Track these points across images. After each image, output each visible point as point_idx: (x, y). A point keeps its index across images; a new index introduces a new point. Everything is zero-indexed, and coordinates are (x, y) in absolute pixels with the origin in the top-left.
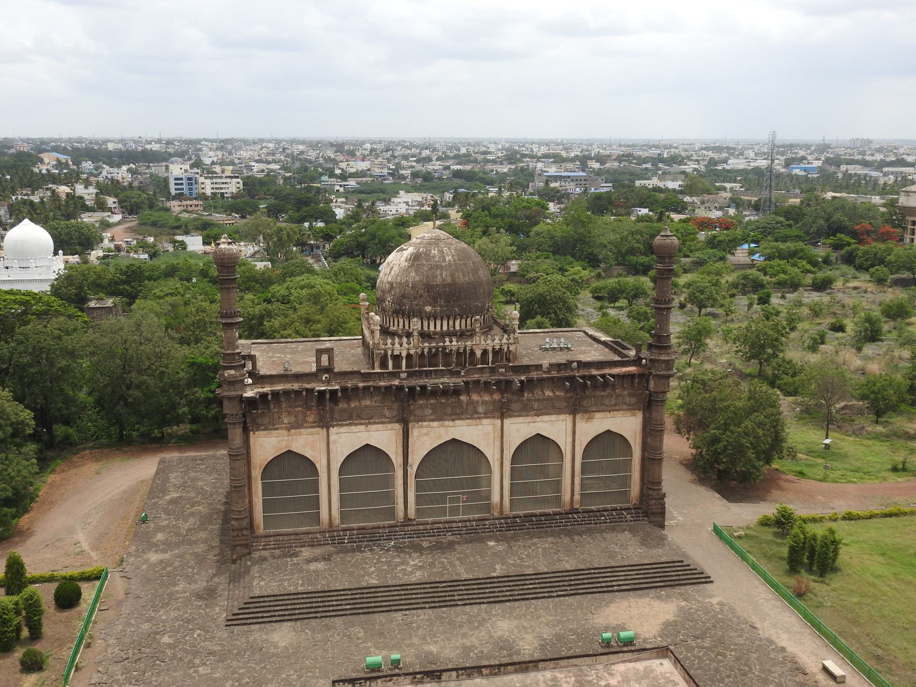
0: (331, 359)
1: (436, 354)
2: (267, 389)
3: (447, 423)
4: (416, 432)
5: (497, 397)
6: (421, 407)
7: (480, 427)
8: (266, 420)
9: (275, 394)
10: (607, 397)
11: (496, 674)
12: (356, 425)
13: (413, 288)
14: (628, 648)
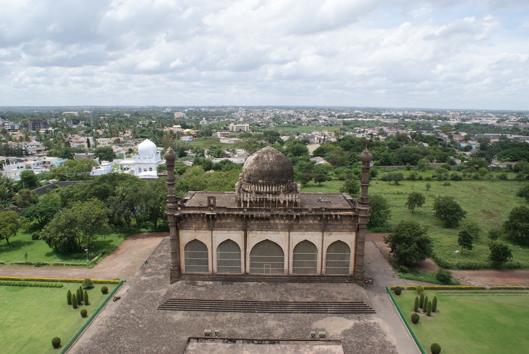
0: (215, 202)
1: (263, 202)
2: (187, 212)
3: (264, 232)
4: (250, 235)
5: (287, 222)
6: (252, 224)
7: (279, 235)
8: (186, 225)
9: (189, 215)
10: (339, 225)
11: (260, 344)
13: (254, 172)
14: (324, 339)
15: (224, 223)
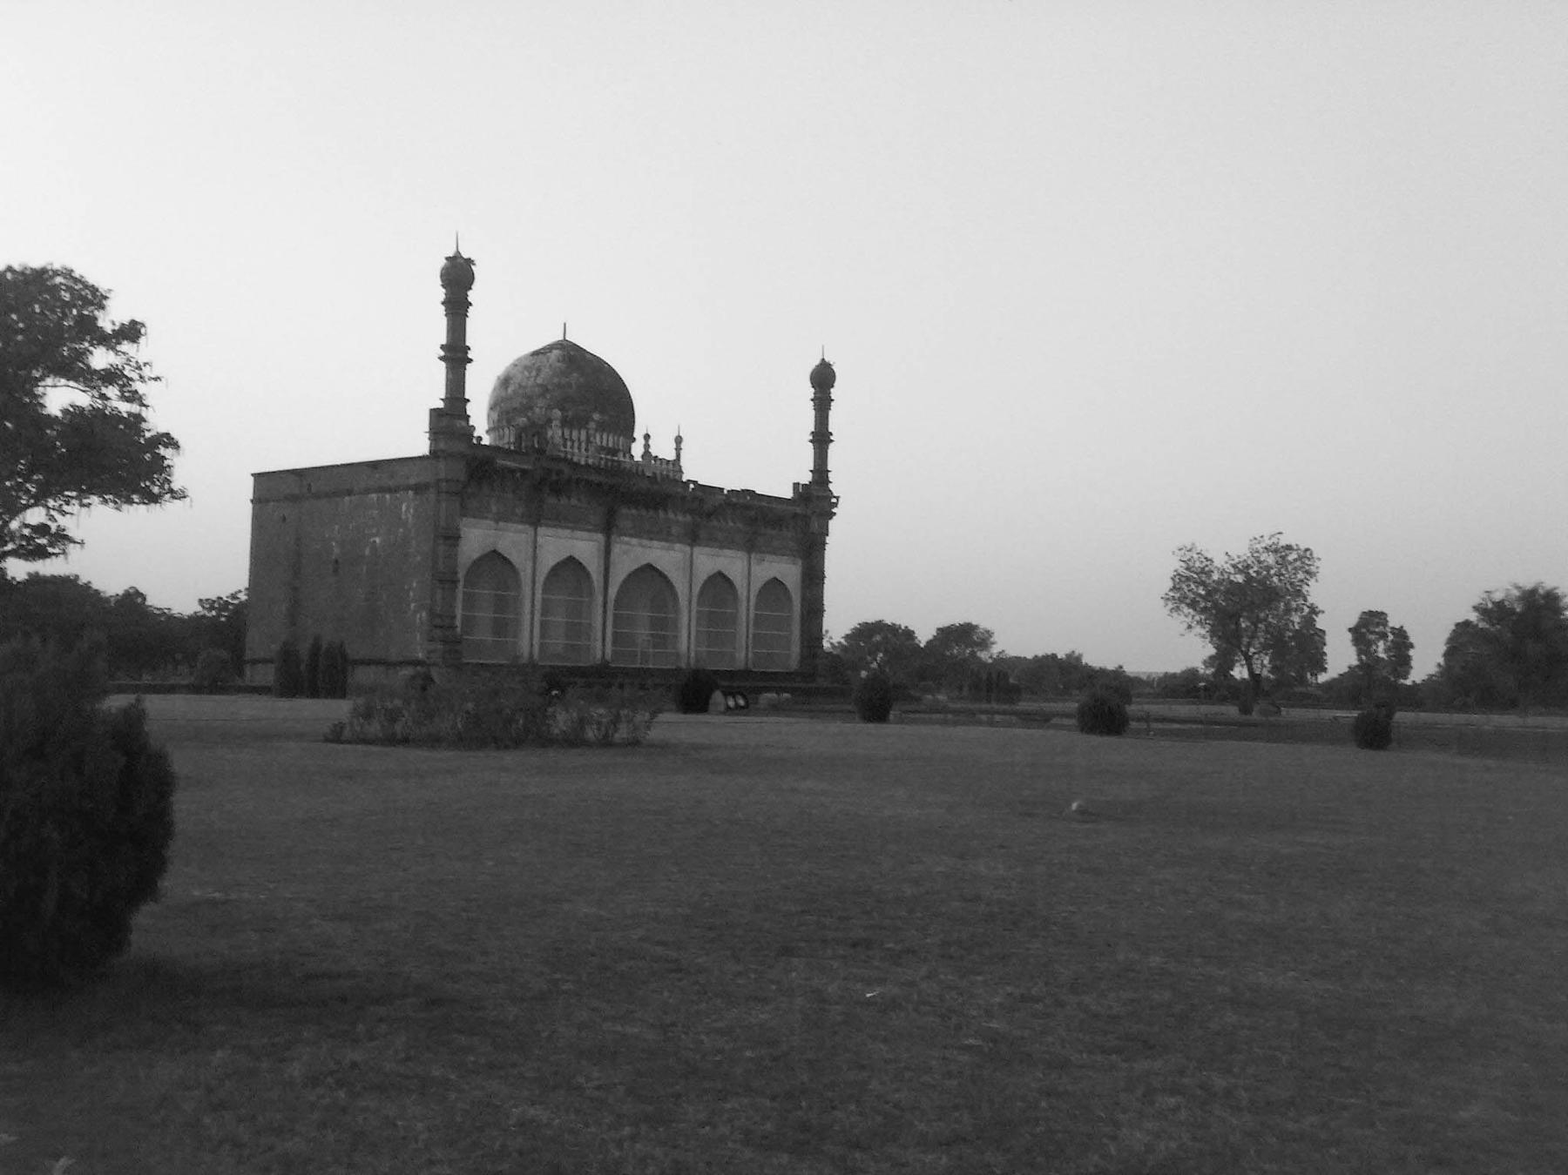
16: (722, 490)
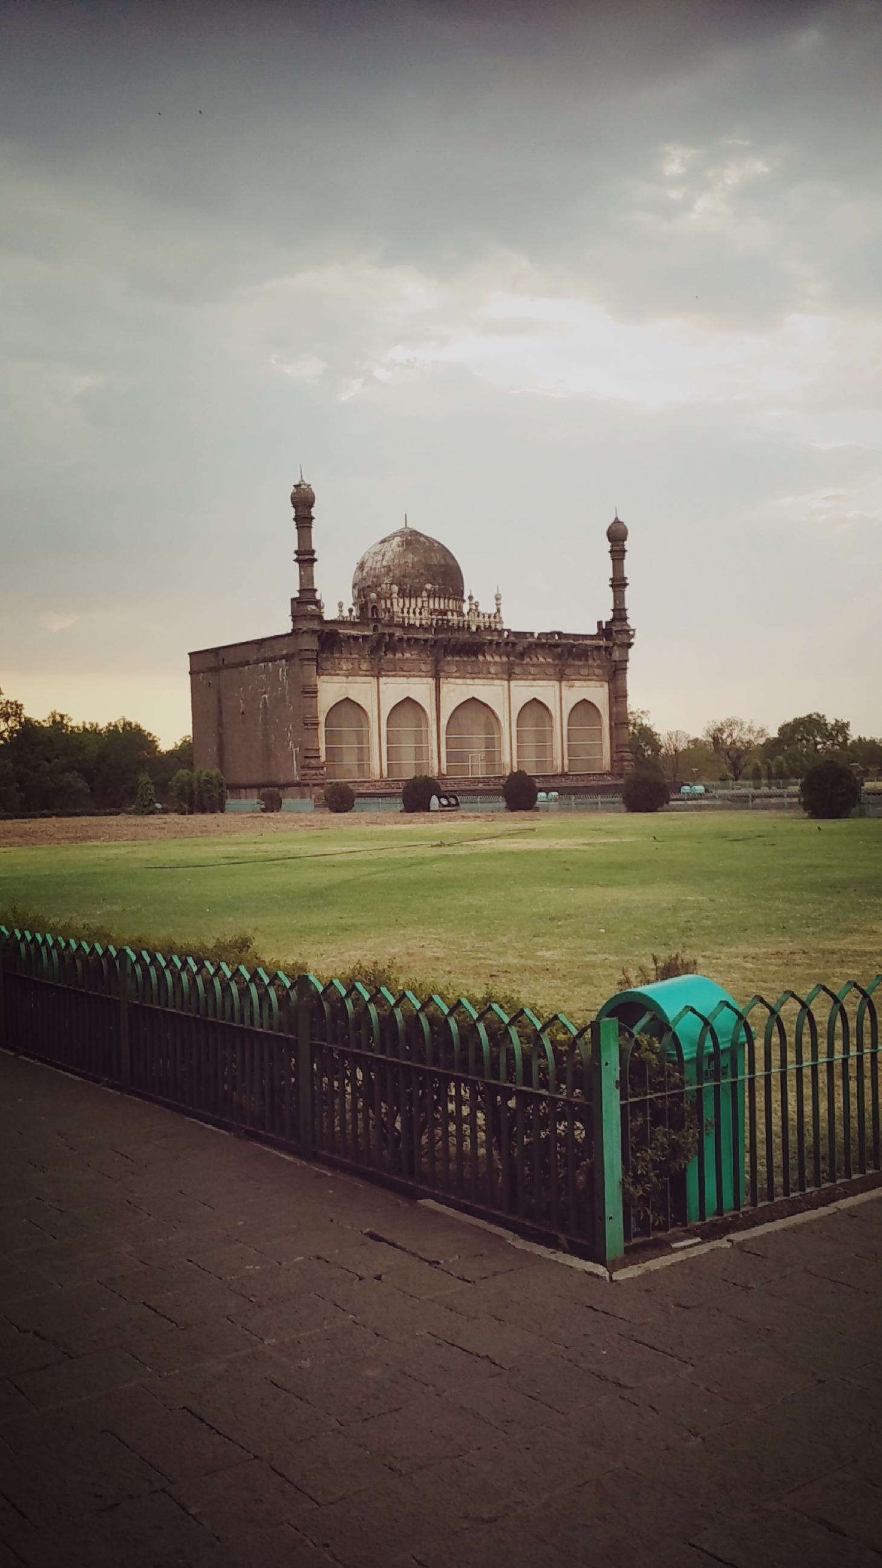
6: (449, 663)
8: (328, 665)
12: (400, 676)
13: (413, 568)
15: (399, 659)
16: (532, 634)
